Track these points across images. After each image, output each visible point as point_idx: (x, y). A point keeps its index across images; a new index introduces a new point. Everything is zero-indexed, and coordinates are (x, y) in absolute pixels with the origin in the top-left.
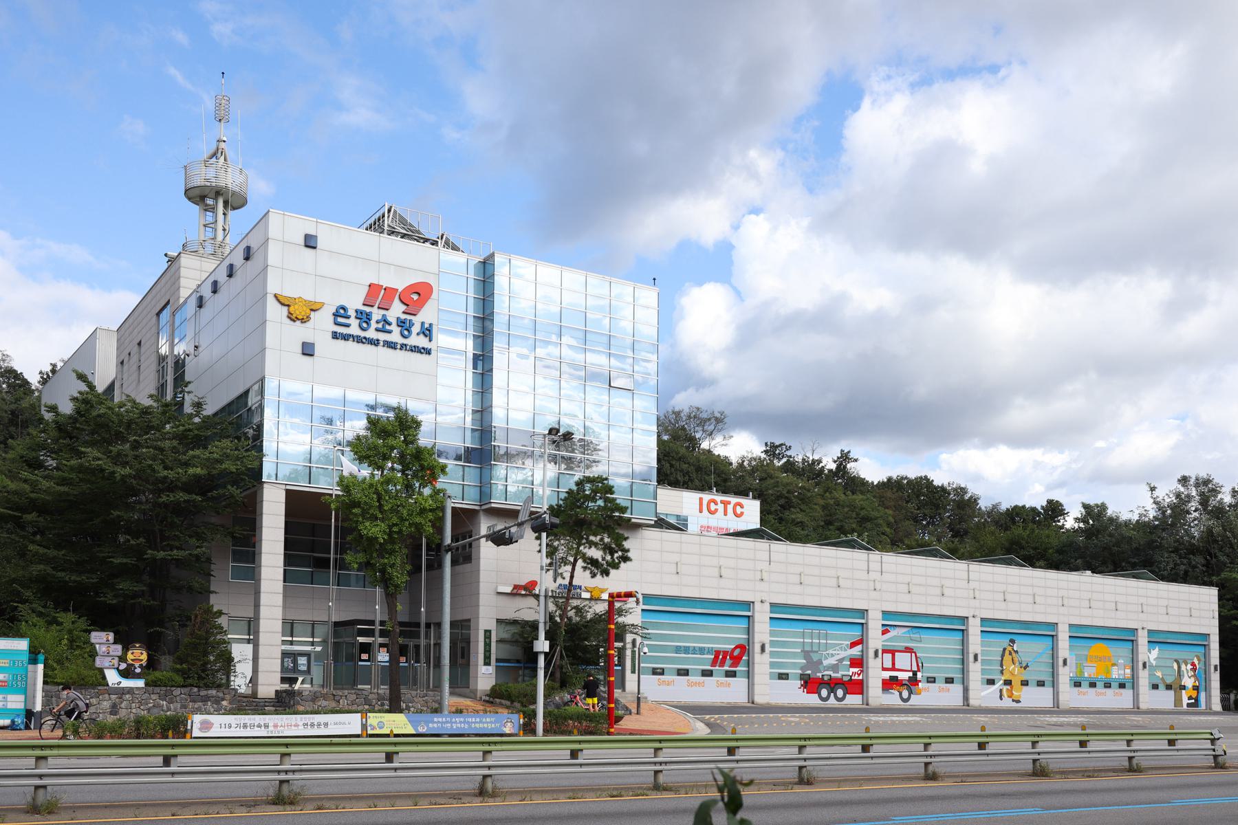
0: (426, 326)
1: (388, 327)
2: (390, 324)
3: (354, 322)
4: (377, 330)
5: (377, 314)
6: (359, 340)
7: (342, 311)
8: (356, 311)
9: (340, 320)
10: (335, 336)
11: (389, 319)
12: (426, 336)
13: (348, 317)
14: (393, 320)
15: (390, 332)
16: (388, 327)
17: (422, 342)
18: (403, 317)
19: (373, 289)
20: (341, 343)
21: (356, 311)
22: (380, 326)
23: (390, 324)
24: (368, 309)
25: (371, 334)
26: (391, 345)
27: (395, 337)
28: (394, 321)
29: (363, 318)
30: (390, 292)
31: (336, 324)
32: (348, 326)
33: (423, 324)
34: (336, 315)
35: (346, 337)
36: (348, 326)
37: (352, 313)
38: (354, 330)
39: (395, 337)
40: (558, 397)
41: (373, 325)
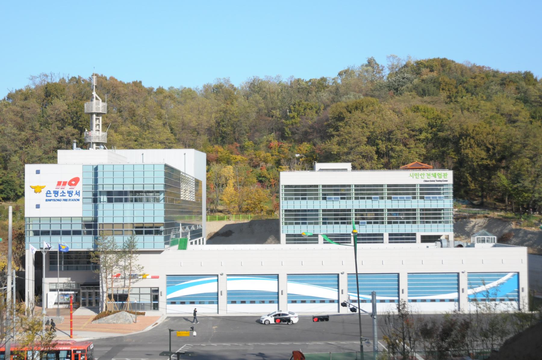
0: (78, 192)
1: (64, 194)
2: (65, 193)
3: (53, 195)
4: (61, 196)
5: (60, 191)
6: (54, 200)
7: (49, 192)
8: (54, 191)
9: (48, 195)
10: (47, 200)
11: (64, 192)
12: (77, 195)
13: (50, 193)
14: (65, 191)
15: (65, 196)
16: (64, 194)
17: (76, 197)
18: (69, 190)
19: (59, 183)
20: (49, 202)
21: (54, 191)
22: (62, 194)
23: (65, 193)
24: (57, 190)
25: (59, 198)
26: (65, 200)
27: (67, 197)
28: (66, 192)
29: (56, 193)
30: (65, 183)
31: (47, 196)
32: (51, 196)
33: (76, 191)
34: (47, 193)
35: (50, 200)
36: (51, 196)
37: (52, 192)
38: (53, 197)
39: (67, 197)
40: (133, 209)
41: (59, 194)
